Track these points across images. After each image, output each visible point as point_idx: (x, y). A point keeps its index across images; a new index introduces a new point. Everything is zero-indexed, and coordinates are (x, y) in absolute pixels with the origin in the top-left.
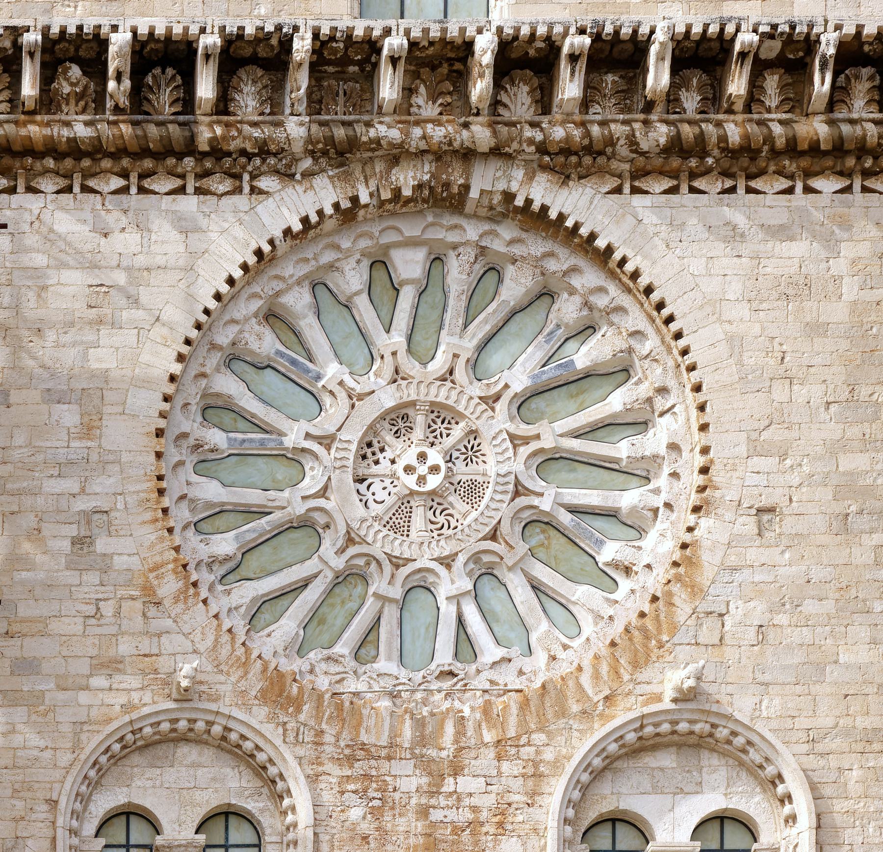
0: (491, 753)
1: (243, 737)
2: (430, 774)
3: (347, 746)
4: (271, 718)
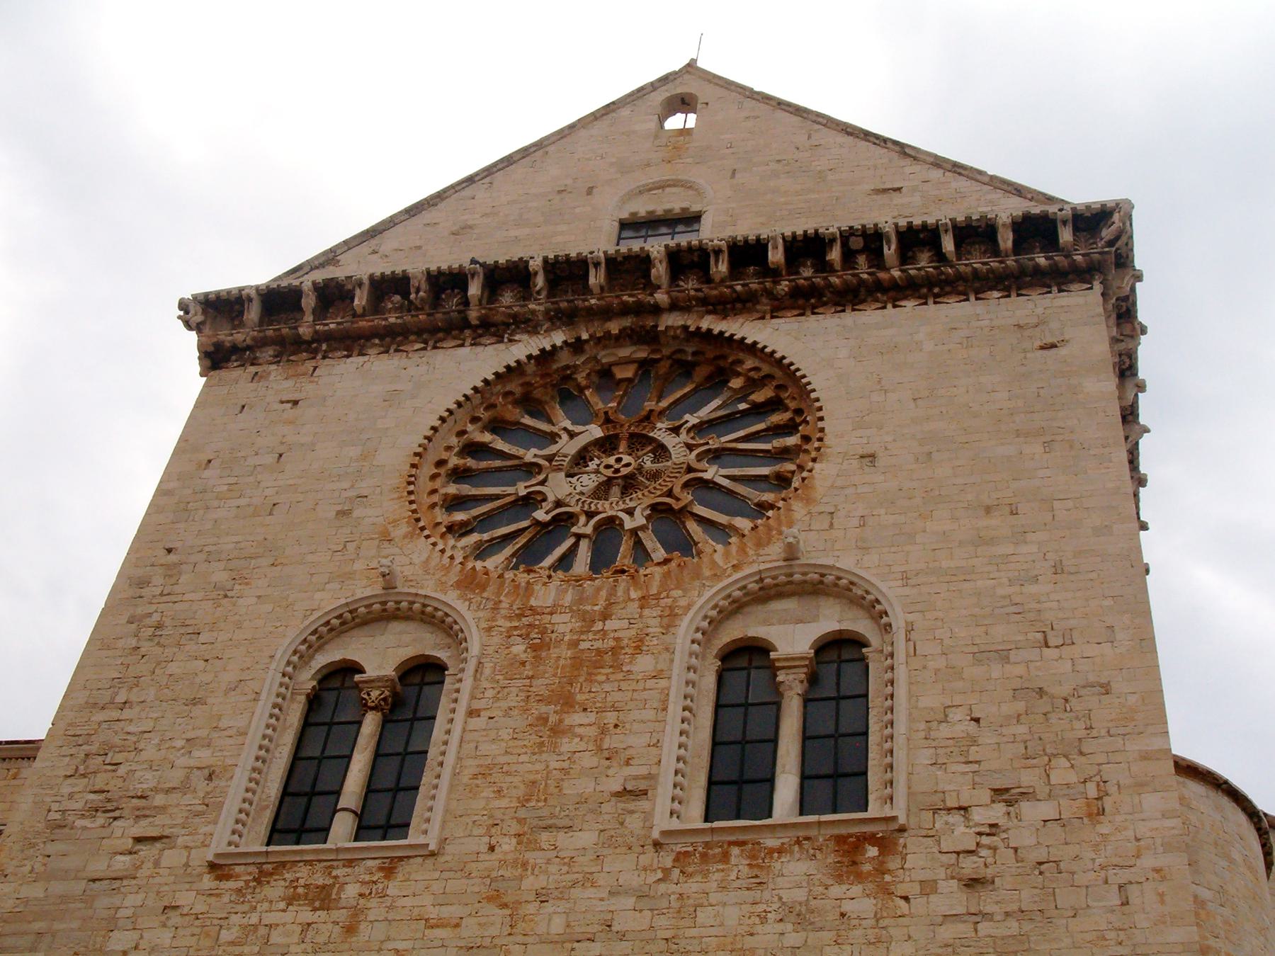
0: (636, 604)
1: (436, 609)
2: (584, 620)
3: (518, 609)
4: (462, 597)
